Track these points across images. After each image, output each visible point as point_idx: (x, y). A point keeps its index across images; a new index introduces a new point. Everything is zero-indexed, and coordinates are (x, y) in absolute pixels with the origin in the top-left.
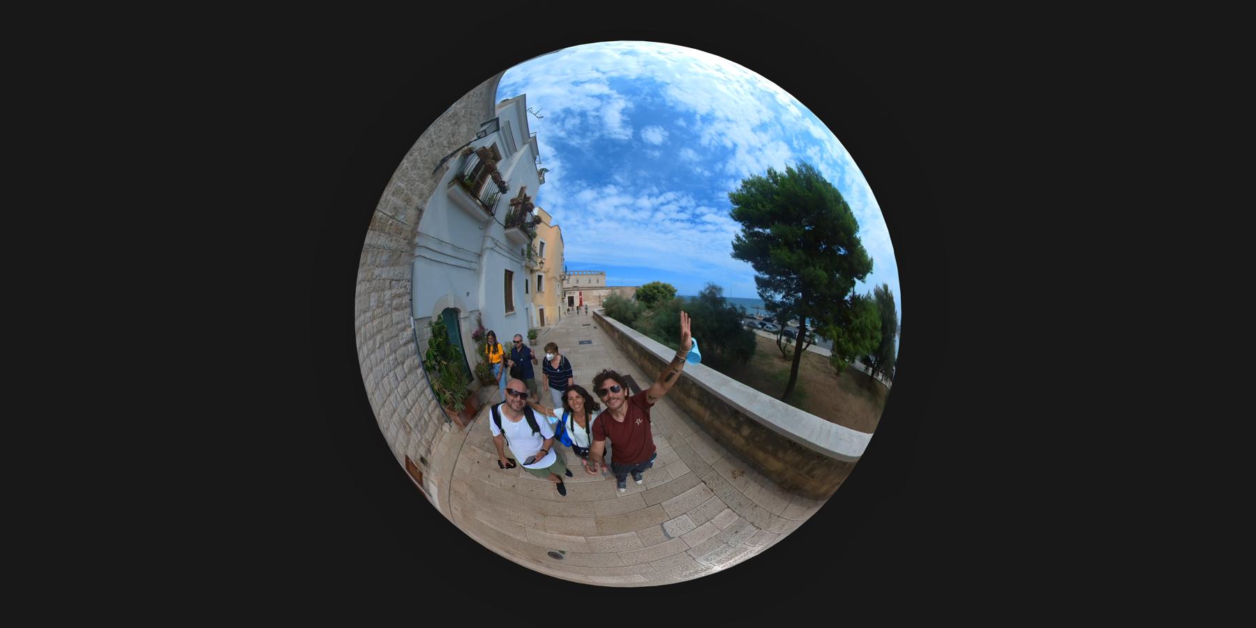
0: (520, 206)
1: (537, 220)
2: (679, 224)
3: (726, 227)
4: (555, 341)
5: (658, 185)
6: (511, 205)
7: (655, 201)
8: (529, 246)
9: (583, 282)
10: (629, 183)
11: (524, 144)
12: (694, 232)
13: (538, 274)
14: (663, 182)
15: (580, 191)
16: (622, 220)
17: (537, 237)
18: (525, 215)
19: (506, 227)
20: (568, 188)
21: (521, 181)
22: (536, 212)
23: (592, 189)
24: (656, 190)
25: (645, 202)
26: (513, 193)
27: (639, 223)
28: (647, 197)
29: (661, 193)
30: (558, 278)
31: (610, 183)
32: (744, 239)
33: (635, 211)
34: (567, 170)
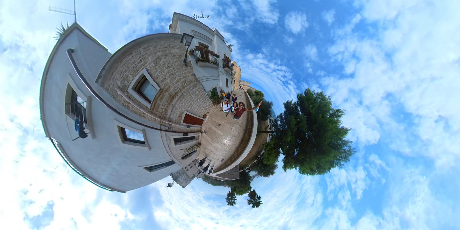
0: (226, 61)
1: (233, 65)
2: (279, 81)
3: (292, 95)
4: (236, 94)
5: (282, 60)
6: (223, 61)
7: (276, 67)
8: (232, 72)
9: (245, 83)
10: (269, 54)
11: (213, 36)
12: (281, 87)
13: (234, 79)
14: (285, 60)
15: (247, 54)
16: (261, 69)
17: (234, 70)
18: (229, 64)
19: (224, 68)
20: (242, 53)
21: (223, 52)
22: (232, 62)
23: (252, 54)
24: (279, 62)
25: (272, 66)
26: (222, 57)
27: (266, 73)
28: (274, 64)
29: (281, 65)
30: (239, 81)
31: (260, 52)
32: (292, 104)
33: (267, 67)
34: (240, 44)
